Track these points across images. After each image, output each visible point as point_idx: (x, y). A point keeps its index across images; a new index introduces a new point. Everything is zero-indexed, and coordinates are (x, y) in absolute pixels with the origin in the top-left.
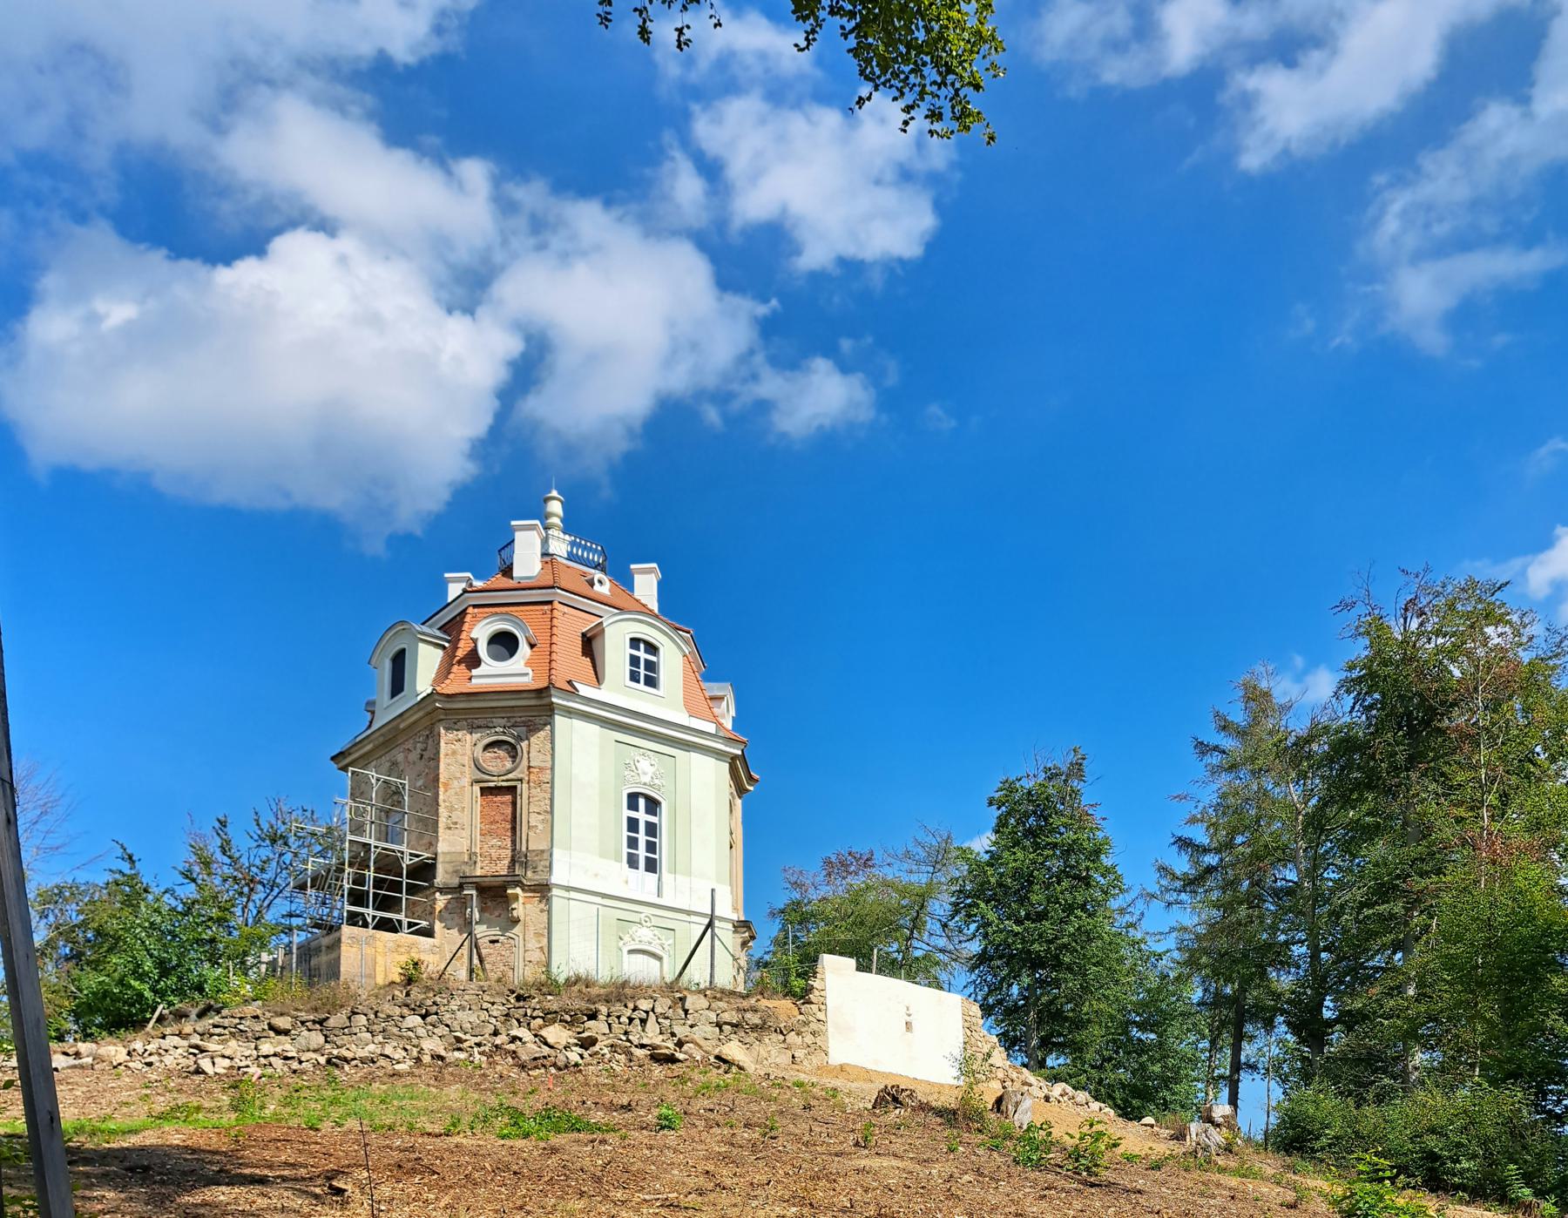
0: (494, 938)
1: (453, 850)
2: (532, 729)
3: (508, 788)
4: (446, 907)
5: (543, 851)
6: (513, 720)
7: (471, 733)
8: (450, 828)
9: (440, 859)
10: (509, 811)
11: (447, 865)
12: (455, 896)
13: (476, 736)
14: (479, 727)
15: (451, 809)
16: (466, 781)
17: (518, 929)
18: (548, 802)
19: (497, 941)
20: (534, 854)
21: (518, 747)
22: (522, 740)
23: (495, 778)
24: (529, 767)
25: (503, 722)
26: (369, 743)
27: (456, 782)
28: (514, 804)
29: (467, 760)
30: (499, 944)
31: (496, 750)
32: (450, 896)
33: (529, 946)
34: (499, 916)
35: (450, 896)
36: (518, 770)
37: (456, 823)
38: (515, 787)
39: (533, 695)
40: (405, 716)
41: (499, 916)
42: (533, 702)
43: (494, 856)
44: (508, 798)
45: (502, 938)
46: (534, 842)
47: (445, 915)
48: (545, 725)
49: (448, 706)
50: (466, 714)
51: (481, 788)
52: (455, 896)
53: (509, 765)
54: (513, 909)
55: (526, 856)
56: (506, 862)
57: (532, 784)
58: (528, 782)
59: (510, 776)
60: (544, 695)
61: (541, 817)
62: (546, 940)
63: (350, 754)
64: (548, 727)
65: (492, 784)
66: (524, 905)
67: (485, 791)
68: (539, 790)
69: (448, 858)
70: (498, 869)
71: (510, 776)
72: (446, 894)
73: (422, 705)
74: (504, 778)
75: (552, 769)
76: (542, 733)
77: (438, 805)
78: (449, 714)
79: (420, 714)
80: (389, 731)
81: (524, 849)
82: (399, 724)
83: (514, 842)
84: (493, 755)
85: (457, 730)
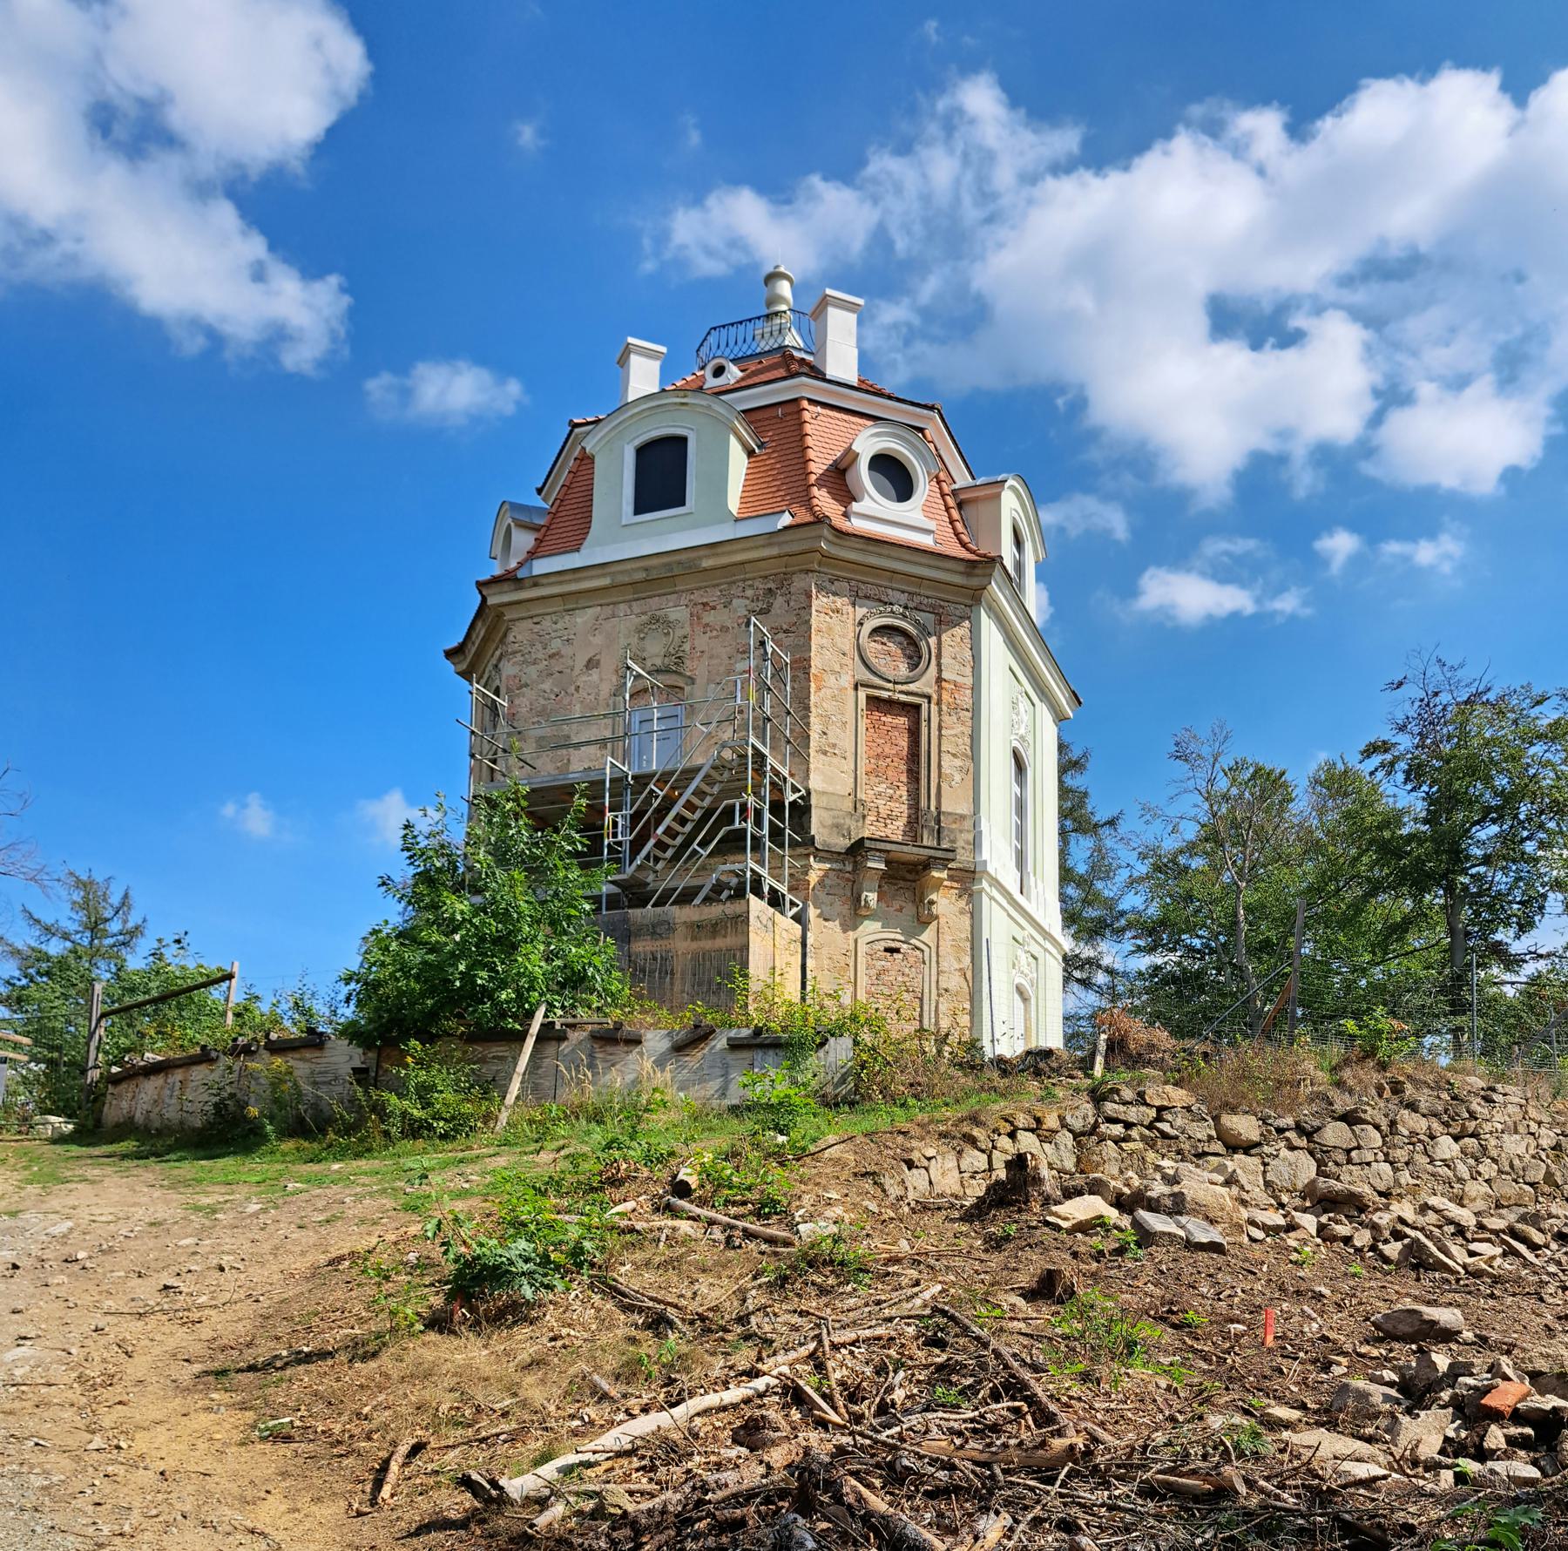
0: (893, 945)
1: (830, 789)
2: (944, 621)
3: (904, 705)
4: (821, 882)
5: (963, 817)
6: (917, 599)
7: (854, 605)
8: (825, 753)
9: (813, 801)
10: (904, 742)
11: (825, 814)
12: (835, 866)
13: (861, 611)
14: (867, 597)
15: (826, 718)
16: (847, 681)
17: (928, 935)
18: (968, 741)
19: (897, 950)
20: (950, 819)
21: (923, 644)
22: (929, 634)
23: (890, 686)
24: (939, 680)
25: (903, 598)
26: (604, 575)
27: (833, 678)
28: (914, 734)
29: (847, 644)
30: (900, 956)
31: (885, 640)
32: (828, 866)
33: (944, 965)
34: (900, 910)
35: (828, 866)
36: (924, 679)
37: (834, 746)
38: (917, 707)
39: (961, 567)
40: (719, 550)
41: (900, 910)
42: (958, 579)
43: (884, 812)
44: (902, 721)
45: (905, 946)
46: (954, 802)
47: (822, 895)
48: (963, 618)
49: (835, 551)
50: (853, 571)
51: (869, 698)
52: (835, 866)
53: (903, 670)
54: (932, 903)
55: (938, 822)
56: (901, 823)
57: (944, 707)
58: (939, 703)
59: (912, 687)
60: (977, 571)
61: (958, 762)
62: (968, 959)
63: (536, 585)
64: (967, 624)
65: (885, 694)
66: (945, 902)
67: (875, 703)
68: (954, 718)
69: (824, 801)
70: (889, 832)
71: (912, 687)
72: (822, 860)
73: (782, 538)
74: (904, 688)
75: (976, 689)
76: (958, 631)
77: (807, 708)
78: (828, 565)
79: (774, 551)
80: (665, 565)
81: (933, 808)
82: (700, 558)
83: (914, 796)
84: (880, 647)
85: (835, 594)
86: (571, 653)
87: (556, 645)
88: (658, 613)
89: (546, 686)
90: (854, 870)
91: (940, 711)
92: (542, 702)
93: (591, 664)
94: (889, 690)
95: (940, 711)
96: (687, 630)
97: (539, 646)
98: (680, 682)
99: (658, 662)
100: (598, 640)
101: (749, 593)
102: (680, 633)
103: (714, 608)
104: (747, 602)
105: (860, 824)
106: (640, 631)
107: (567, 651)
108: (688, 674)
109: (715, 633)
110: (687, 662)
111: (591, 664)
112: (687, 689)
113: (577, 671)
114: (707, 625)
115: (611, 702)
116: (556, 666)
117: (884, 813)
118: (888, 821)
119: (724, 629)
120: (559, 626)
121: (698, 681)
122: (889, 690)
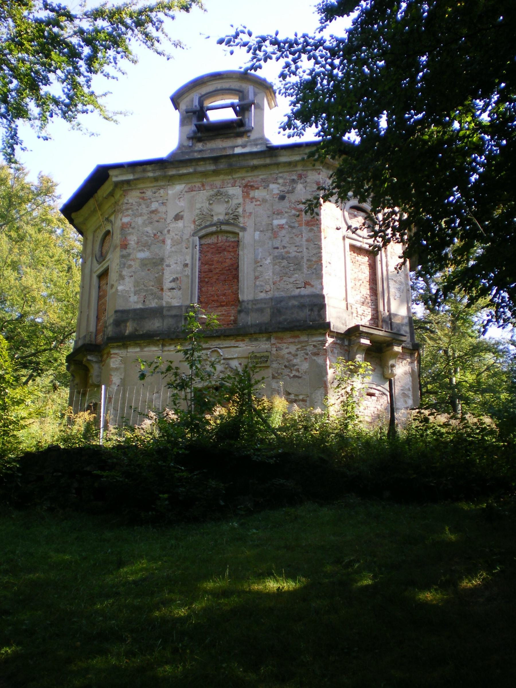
86: (164, 210)
87: (154, 206)
88: (221, 190)
89: (149, 229)
90: (349, 344)
91: (386, 256)
92: (146, 238)
93: (178, 217)
94: (361, 242)
95: (386, 256)
96: (241, 200)
97: (144, 206)
98: (237, 230)
99: (221, 217)
100: (182, 204)
101: (281, 181)
102: (235, 202)
103: (258, 188)
104: (278, 186)
105: (351, 317)
106: (211, 200)
107: (162, 209)
108: (241, 225)
109: (258, 203)
110: (241, 219)
111: (178, 217)
112: (241, 234)
113: (168, 221)
114: (253, 198)
115: (191, 240)
116: (155, 217)
117: (360, 312)
118: (363, 317)
119: (264, 201)
120: (157, 195)
121: (248, 229)
122: (361, 242)
